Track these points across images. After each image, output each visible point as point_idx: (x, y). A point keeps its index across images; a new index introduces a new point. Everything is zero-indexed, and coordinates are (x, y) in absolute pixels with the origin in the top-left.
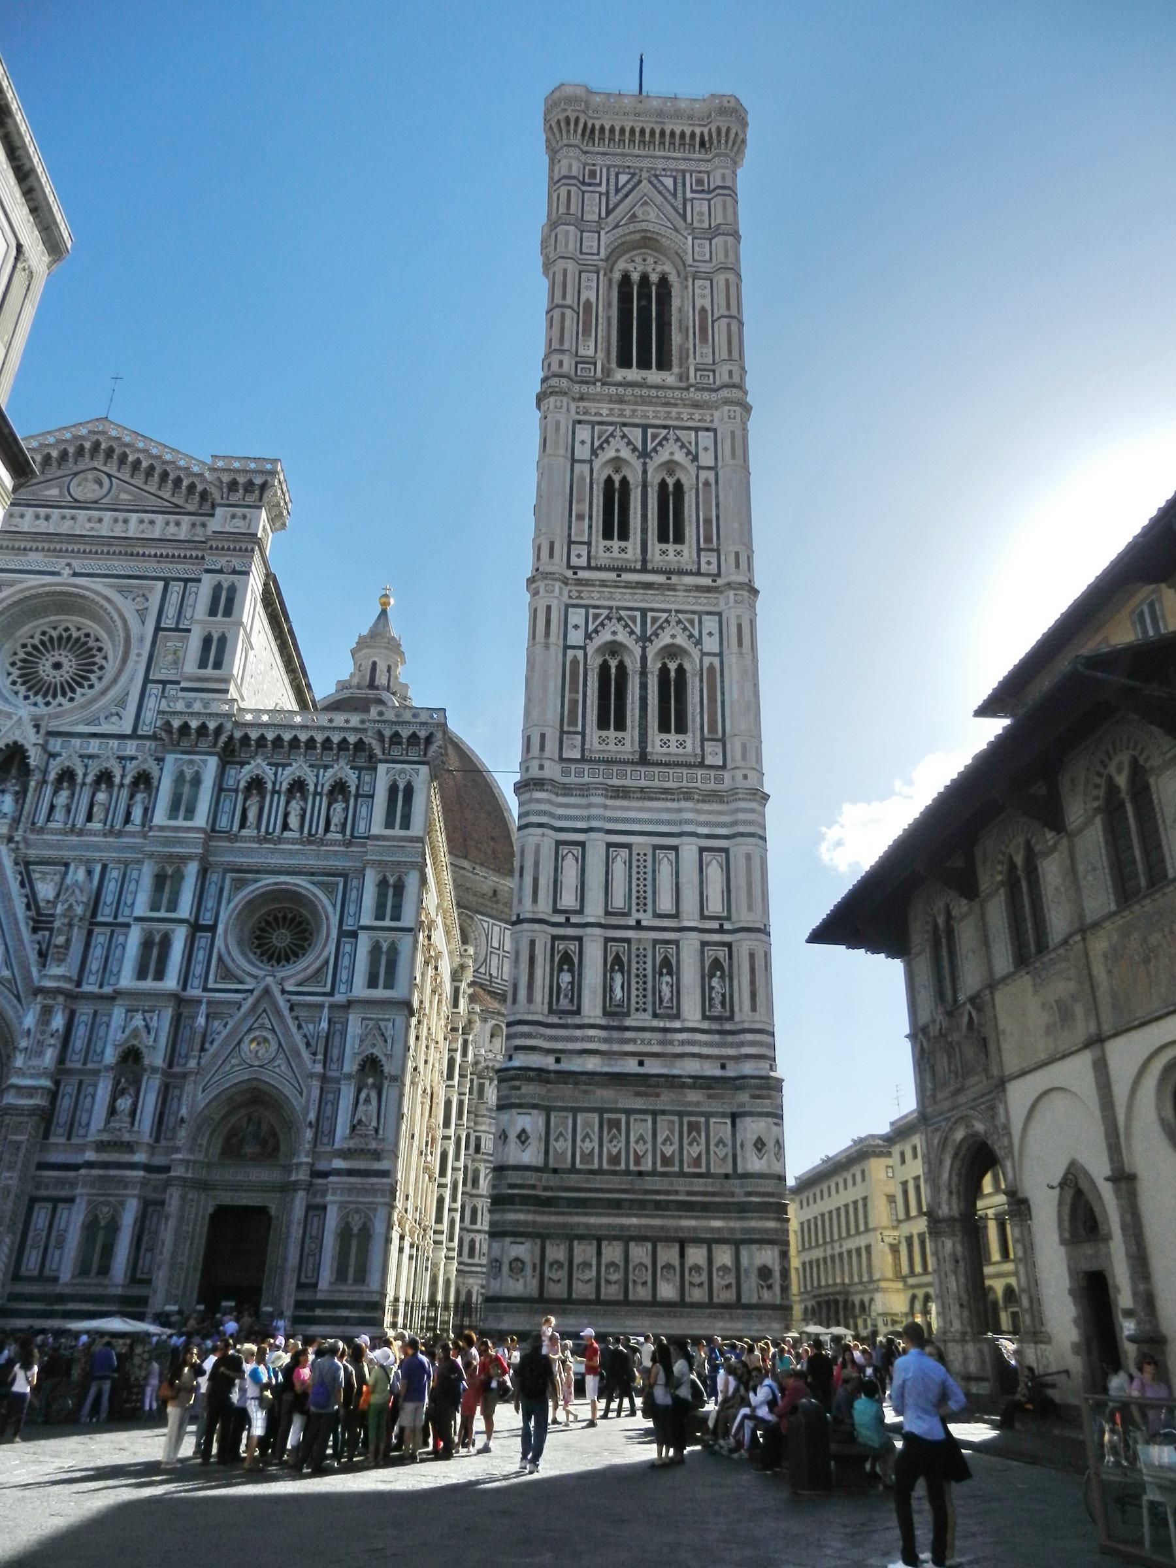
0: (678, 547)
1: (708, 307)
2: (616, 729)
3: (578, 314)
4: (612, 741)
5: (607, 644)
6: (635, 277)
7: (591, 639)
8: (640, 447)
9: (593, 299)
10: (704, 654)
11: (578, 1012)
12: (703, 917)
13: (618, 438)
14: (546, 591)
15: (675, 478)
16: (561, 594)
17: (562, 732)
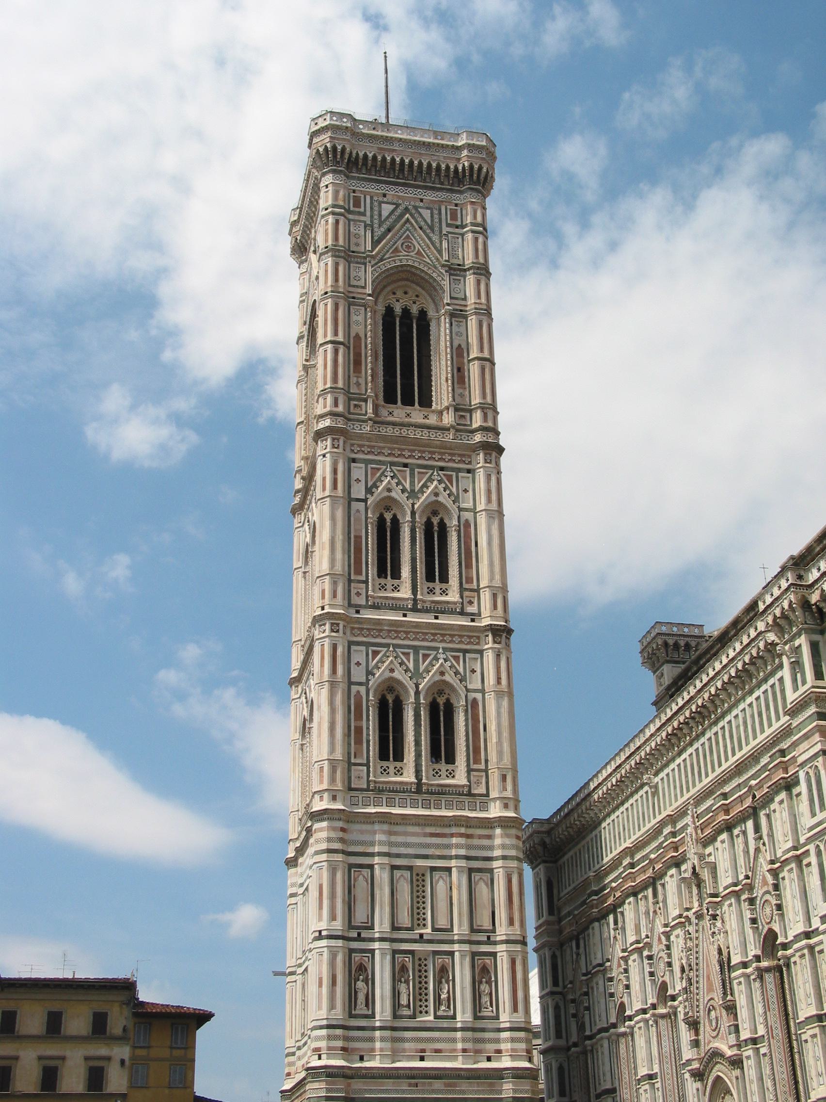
0: (444, 586)
1: (464, 346)
2: (395, 760)
3: (349, 348)
4: (392, 770)
5: (384, 682)
6: (398, 310)
7: (374, 675)
8: (408, 486)
9: (362, 336)
10: (468, 690)
11: (373, 1016)
12: (473, 930)
13: (389, 478)
14: (332, 631)
15: (439, 516)
16: (344, 633)
17: (350, 764)
